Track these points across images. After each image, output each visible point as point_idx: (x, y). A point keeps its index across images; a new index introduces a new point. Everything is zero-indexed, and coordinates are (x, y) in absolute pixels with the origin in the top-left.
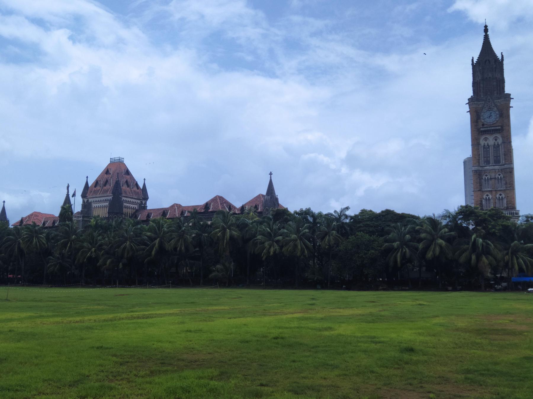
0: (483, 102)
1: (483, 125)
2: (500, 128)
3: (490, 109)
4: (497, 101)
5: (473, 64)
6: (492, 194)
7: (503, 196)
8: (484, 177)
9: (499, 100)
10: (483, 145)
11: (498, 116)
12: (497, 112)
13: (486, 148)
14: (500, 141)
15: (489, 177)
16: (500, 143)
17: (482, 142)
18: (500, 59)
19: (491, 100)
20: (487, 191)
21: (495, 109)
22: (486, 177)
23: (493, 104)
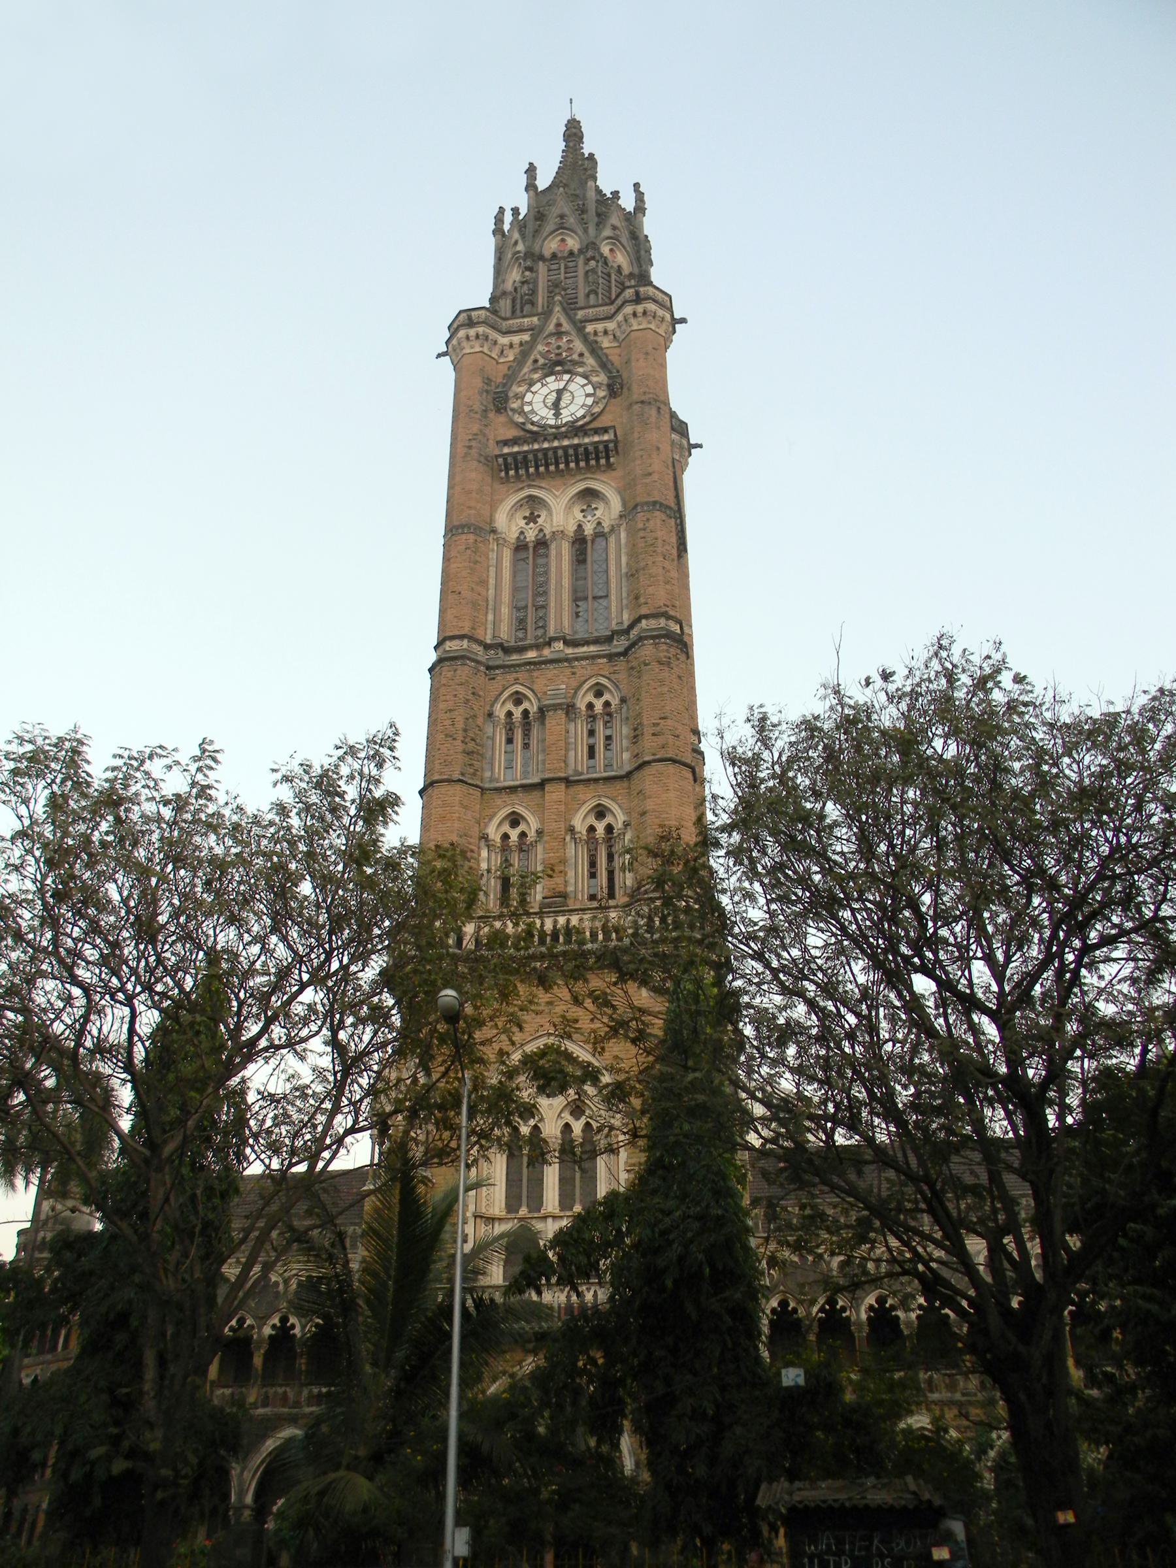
0: (526, 337)
3: (556, 365)
4: (600, 327)
5: (498, 231)
6: (540, 810)
7: (618, 818)
8: (500, 712)
9: (611, 325)
10: (513, 535)
11: (601, 393)
13: (532, 551)
14: (611, 509)
15: (532, 707)
16: (606, 525)
17: (509, 522)
18: (627, 202)
19: (566, 326)
20: (512, 789)
21: (590, 361)
22: (517, 713)
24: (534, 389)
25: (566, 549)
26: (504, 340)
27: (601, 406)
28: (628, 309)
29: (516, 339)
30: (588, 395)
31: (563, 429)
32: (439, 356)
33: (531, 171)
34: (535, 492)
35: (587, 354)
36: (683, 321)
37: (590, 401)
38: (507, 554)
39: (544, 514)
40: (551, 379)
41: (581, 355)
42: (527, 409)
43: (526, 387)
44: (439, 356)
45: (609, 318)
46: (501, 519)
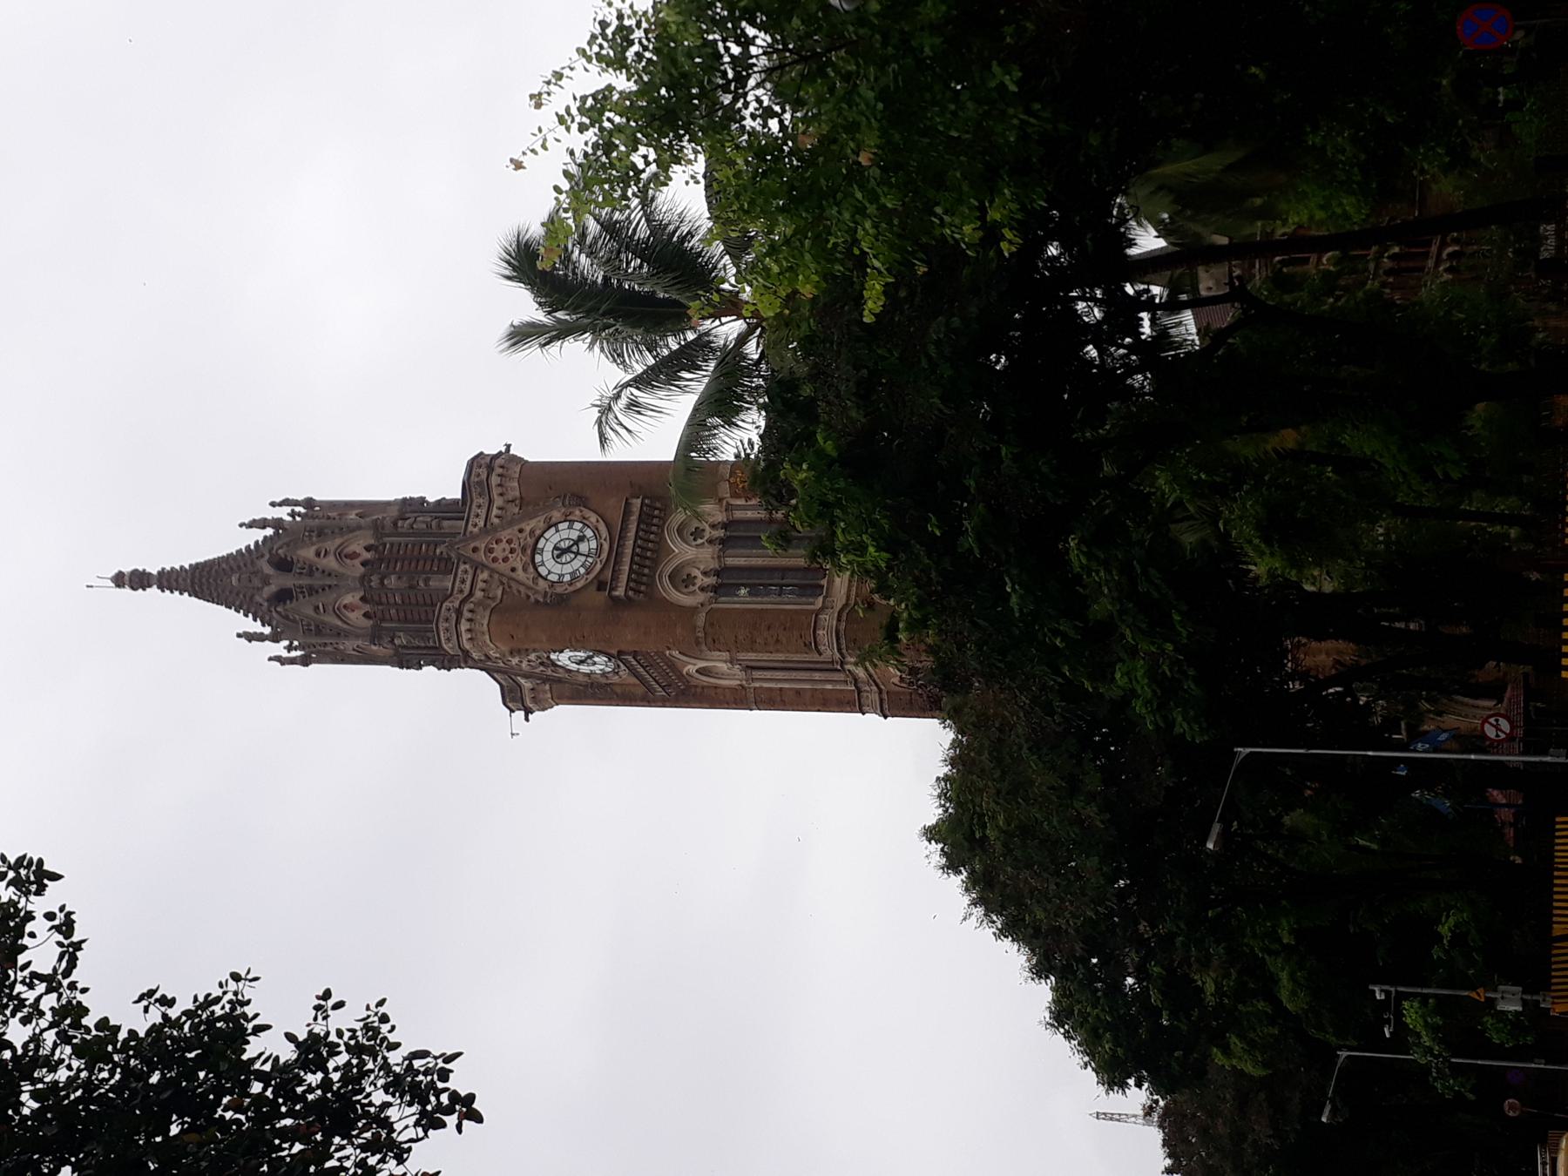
1: (601, 586)
2: (637, 502)
4: (495, 511)
9: (498, 501)
12: (556, 515)
16: (720, 517)
23: (504, 535)
26: (479, 594)
29: (480, 585)
30: (570, 527)
31: (606, 546)
34: (669, 569)
35: (523, 525)
36: (508, 447)
37: (578, 526)
39: (687, 570)
40: (538, 558)
41: (521, 531)
42: (567, 578)
43: (541, 581)
45: (491, 501)
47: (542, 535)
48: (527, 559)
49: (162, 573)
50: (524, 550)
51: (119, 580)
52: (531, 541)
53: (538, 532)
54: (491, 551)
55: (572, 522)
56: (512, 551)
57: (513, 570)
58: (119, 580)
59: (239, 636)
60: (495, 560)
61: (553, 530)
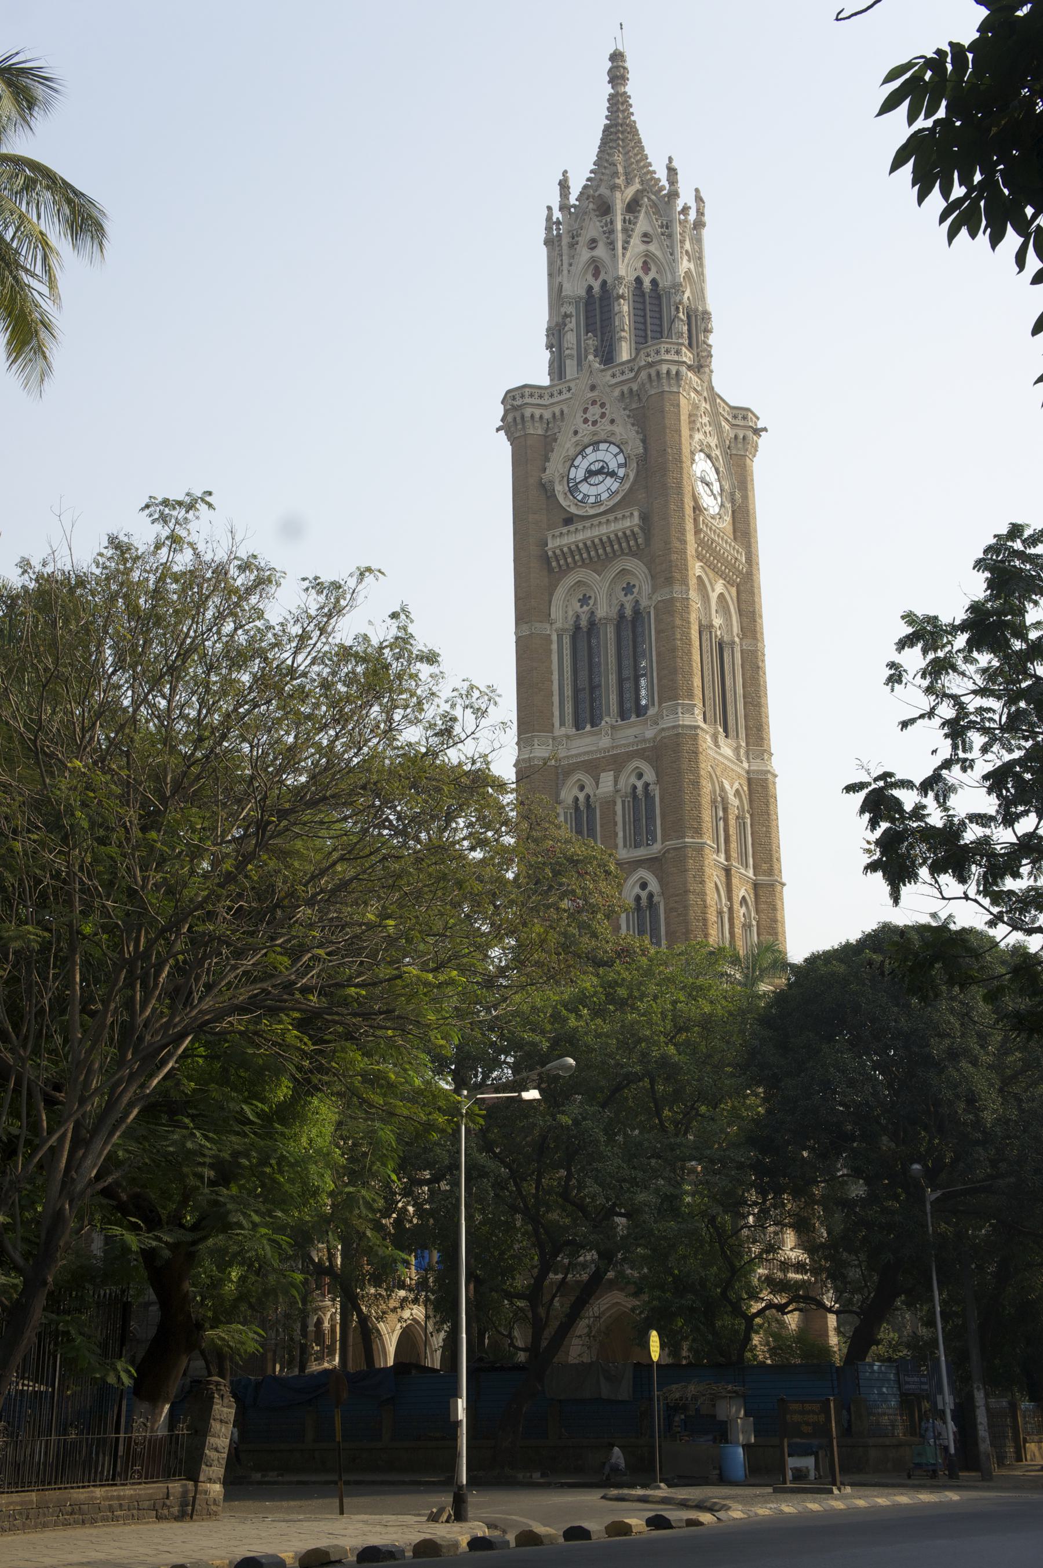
1: (569, 520)
24: (576, 463)
25: (611, 632)
27: (632, 476)
28: (643, 375)
31: (602, 509)
32: (498, 430)
33: (564, 186)
38: (567, 640)
44: (498, 430)
46: (557, 612)
47: (611, 443)
48: (586, 440)
49: (626, 96)
50: (595, 434)
51: (617, 57)
52: (603, 436)
53: (611, 439)
54: (594, 403)
55: (625, 465)
56: (595, 423)
57: (576, 433)
58: (617, 57)
59: (549, 208)
60: (585, 410)
61: (615, 450)
